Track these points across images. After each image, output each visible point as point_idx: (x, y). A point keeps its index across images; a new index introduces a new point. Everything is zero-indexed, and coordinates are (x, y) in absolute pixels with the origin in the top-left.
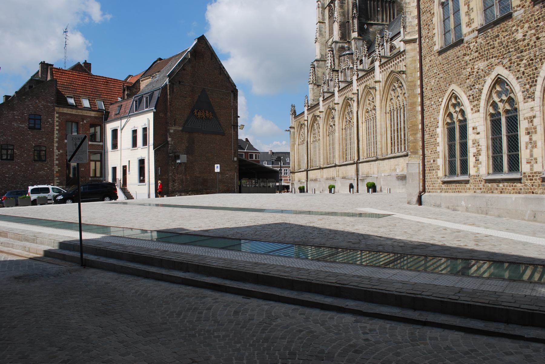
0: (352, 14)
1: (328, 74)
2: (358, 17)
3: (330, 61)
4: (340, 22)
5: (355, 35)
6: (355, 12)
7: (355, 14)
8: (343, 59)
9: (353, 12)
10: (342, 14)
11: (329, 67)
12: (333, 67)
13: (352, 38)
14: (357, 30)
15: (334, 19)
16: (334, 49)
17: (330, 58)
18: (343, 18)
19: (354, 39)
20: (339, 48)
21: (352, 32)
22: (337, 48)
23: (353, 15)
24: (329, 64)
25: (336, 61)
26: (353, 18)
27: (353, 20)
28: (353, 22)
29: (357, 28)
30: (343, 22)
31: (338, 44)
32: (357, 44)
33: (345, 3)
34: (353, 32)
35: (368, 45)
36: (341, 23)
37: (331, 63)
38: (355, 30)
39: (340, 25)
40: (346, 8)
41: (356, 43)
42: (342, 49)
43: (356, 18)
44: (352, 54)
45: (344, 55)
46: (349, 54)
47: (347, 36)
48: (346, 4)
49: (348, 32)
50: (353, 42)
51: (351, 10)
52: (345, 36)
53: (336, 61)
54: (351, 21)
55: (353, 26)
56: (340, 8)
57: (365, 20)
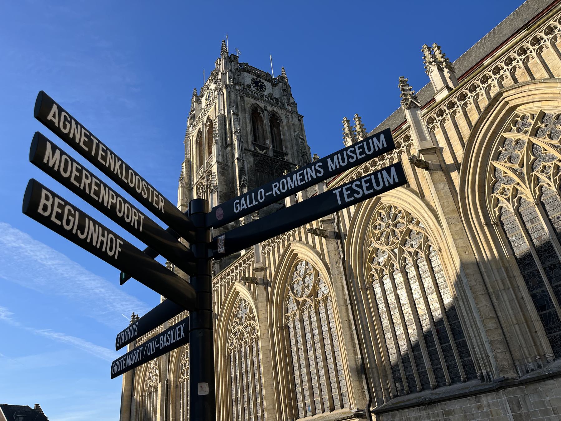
4: (220, 191)
10: (223, 183)
18: (226, 187)
36: (222, 193)
56: (220, 174)
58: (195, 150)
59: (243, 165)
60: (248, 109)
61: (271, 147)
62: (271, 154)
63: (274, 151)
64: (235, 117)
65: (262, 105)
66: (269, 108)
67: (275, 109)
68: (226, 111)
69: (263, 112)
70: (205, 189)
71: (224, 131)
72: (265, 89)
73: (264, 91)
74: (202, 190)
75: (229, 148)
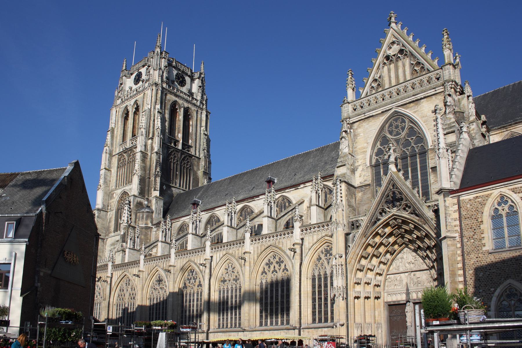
0: (155, 172)
1: (124, 229)
2: (161, 175)
3: (126, 215)
4: (140, 176)
5: (157, 193)
6: (158, 170)
7: (158, 172)
8: (141, 215)
9: (156, 169)
10: (143, 169)
11: (126, 221)
12: (129, 223)
13: (153, 196)
14: (159, 189)
15: (135, 172)
16: (132, 204)
17: (127, 211)
19: (156, 197)
20: (137, 203)
21: (153, 189)
22: (135, 203)
23: (157, 173)
24: (126, 219)
25: (133, 217)
26: (156, 176)
27: (155, 178)
28: (155, 180)
29: (159, 187)
30: (143, 177)
31: (137, 198)
32: (158, 203)
33: (147, 158)
34: (155, 190)
35: (165, 207)
37: (128, 217)
38: (156, 189)
39: (140, 179)
40: (148, 163)
41: (157, 202)
42: (139, 205)
43: (159, 176)
44: (153, 212)
45: (143, 212)
46: (147, 212)
47: (146, 192)
48: (149, 159)
49: (148, 188)
50: (154, 201)
51: (154, 167)
52: (144, 191)
53: (133, 217)
54: (152, 178)
55: (155, 184)
57: (164, 180)
58: (120, 123)
59: (160, 158)
60: (168, 106)
61: (181, 141)
62: (180, 147)
63: (183, 144)
64: (159, 115)
65: (180, 102)
66: (186, 105)
67: (190, 106)
68: (153, 107)
69: (180, 109)
70: (125, 161)
71: (148, 124)
72: (185, 84)
73: (184, 86)
74: (123, 162)
75: (150, 141)
